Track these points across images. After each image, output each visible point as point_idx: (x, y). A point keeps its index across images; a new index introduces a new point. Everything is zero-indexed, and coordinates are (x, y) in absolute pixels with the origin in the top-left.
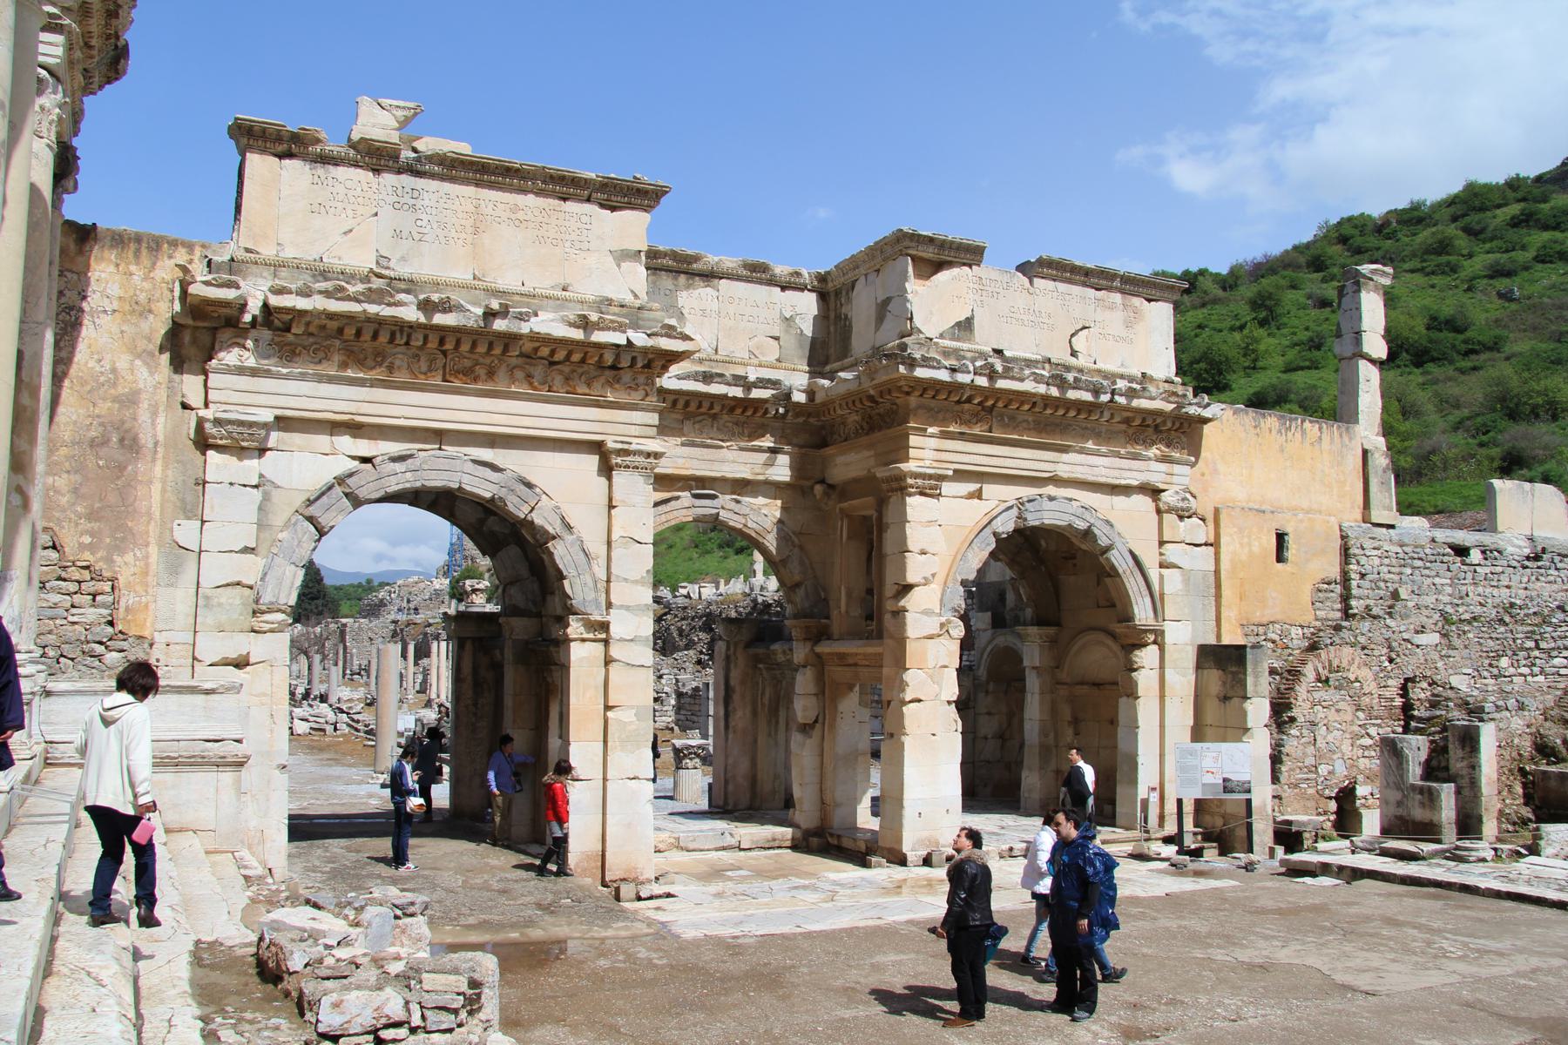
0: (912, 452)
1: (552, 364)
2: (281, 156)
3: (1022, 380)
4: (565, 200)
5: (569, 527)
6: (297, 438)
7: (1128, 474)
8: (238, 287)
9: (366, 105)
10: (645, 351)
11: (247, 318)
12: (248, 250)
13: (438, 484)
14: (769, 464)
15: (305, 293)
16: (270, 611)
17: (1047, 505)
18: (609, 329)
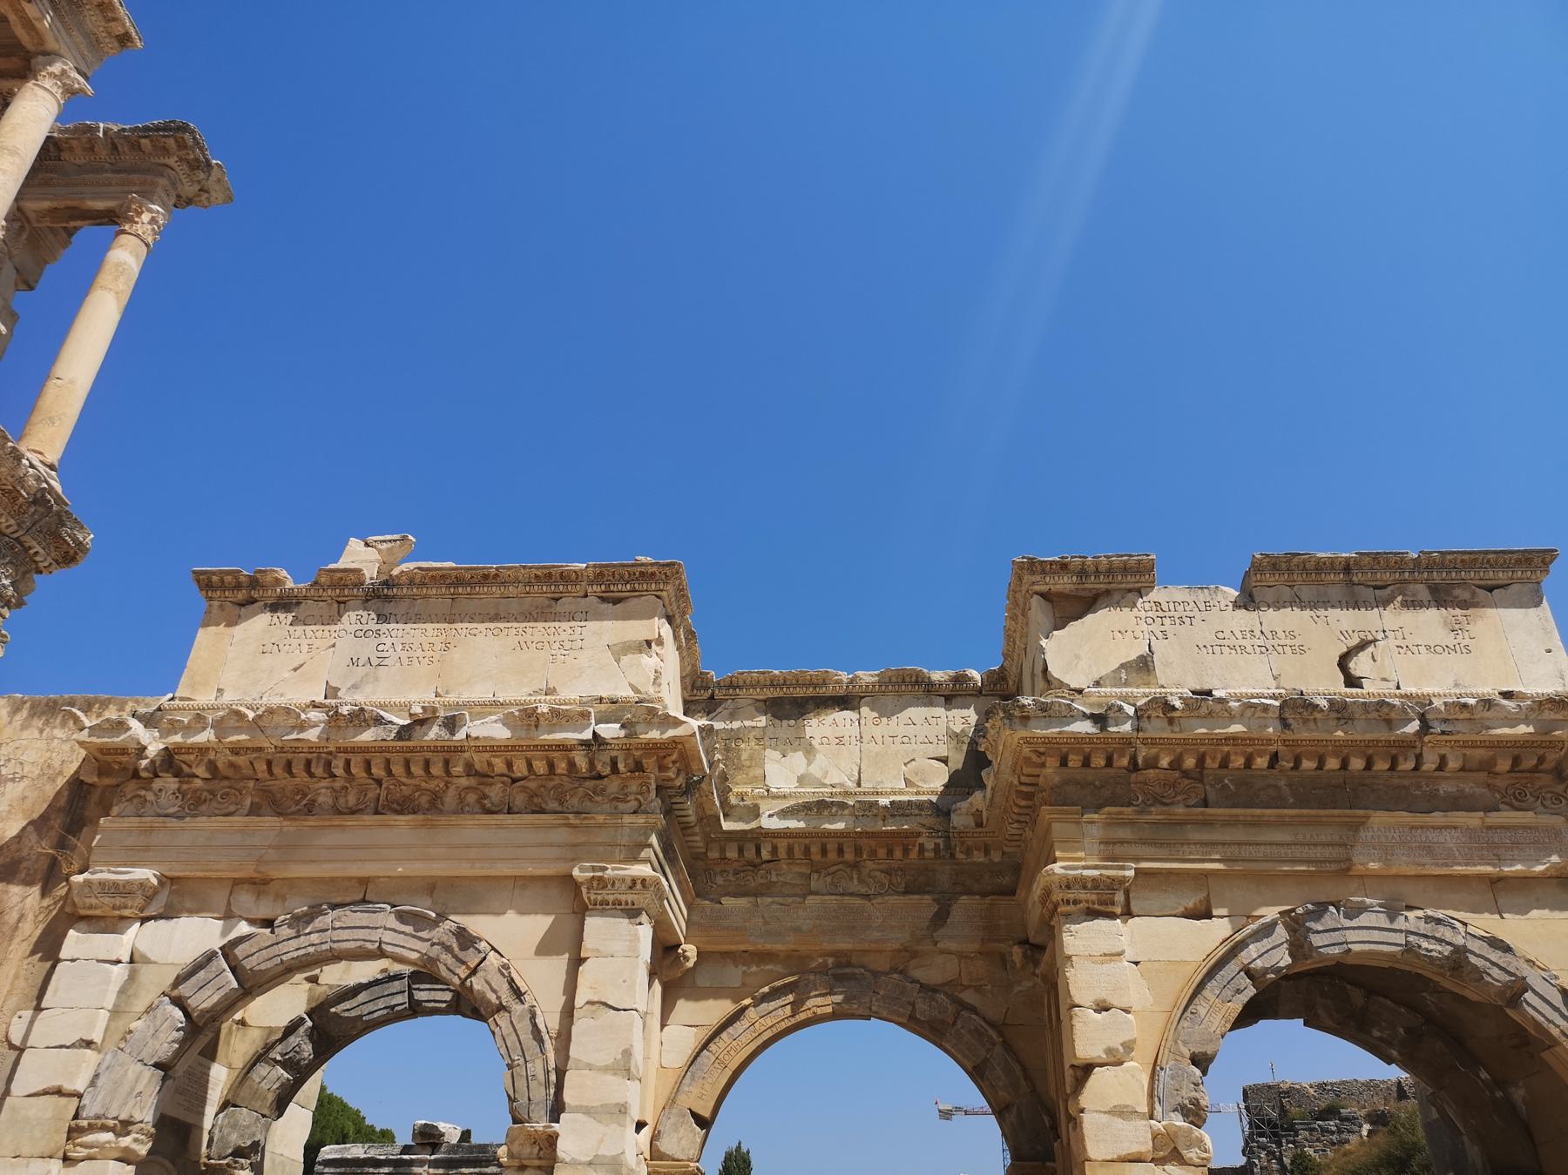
1: (514, 781)
5: (518, 994)
9: (355, 544)
16: (92, 1128)
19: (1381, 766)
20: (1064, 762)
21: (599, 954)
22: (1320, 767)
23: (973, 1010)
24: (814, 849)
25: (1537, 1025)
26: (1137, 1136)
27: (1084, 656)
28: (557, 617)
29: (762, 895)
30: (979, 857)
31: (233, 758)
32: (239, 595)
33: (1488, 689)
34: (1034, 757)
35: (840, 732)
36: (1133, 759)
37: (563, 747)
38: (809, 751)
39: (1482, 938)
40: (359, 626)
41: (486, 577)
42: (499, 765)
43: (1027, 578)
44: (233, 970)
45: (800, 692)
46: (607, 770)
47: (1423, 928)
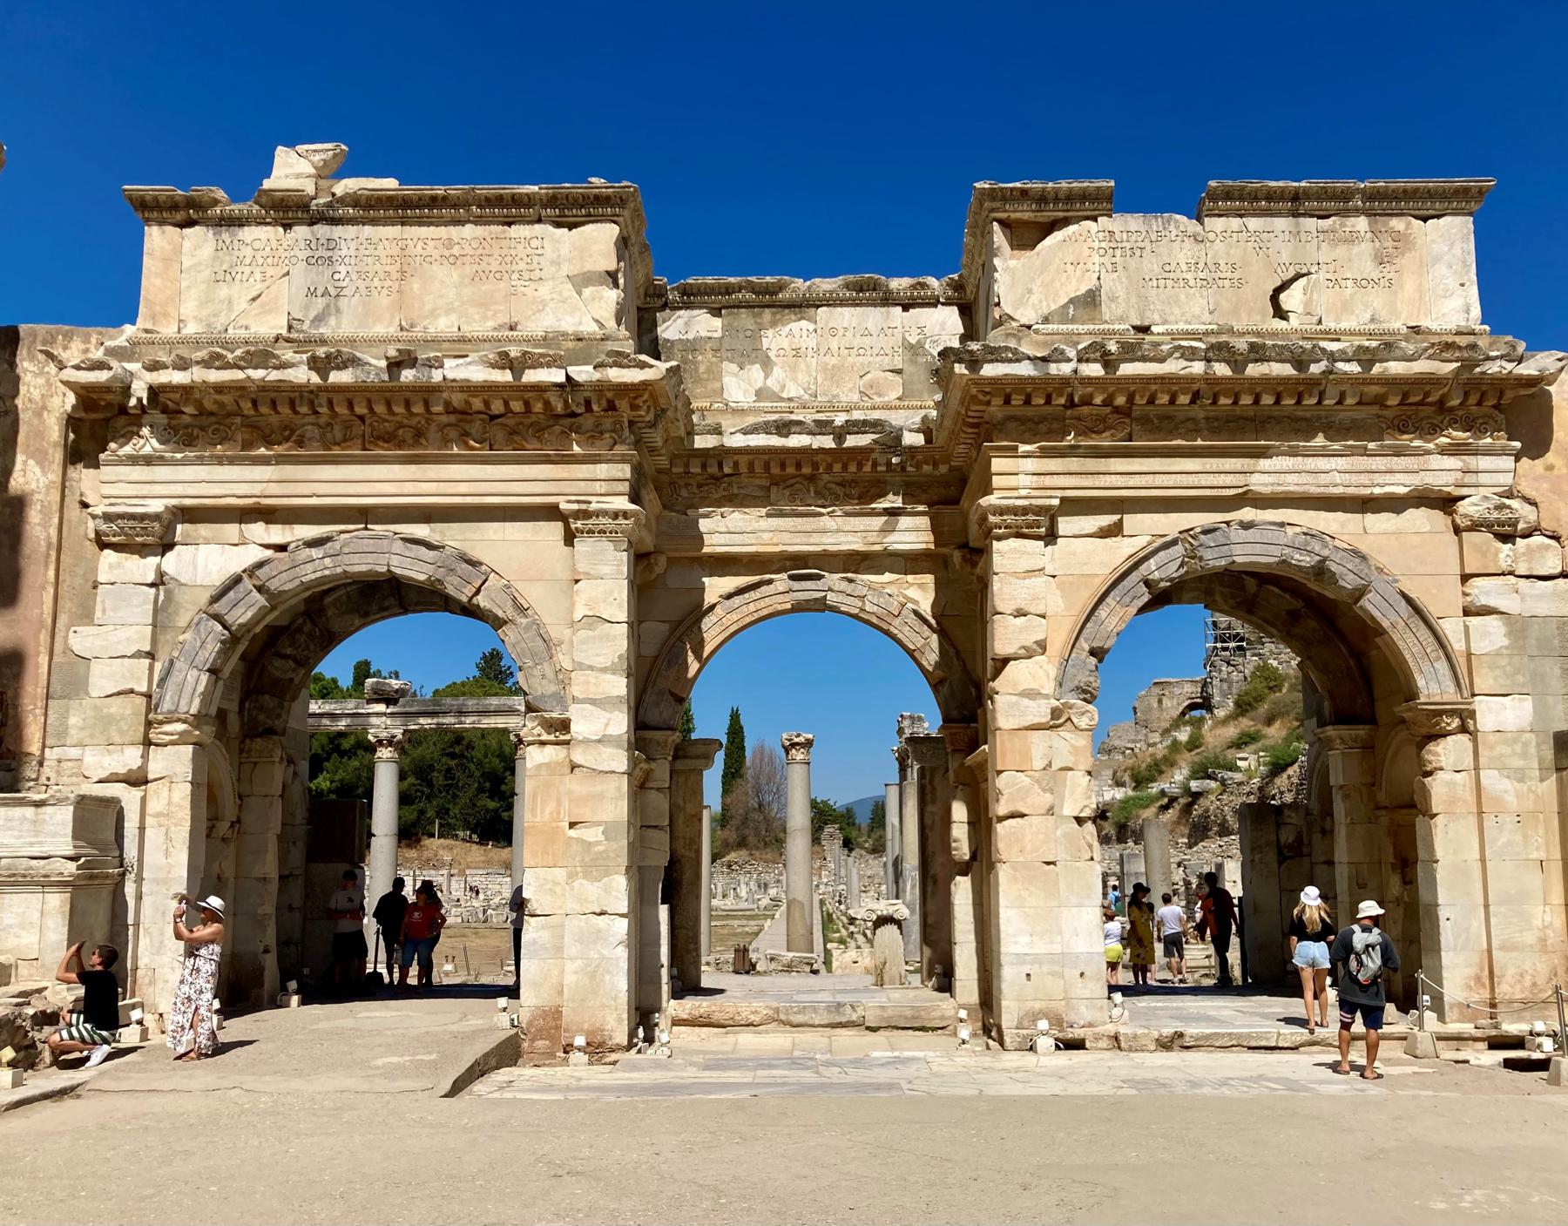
0: (997, 481)
1: (493, 418)
2: (182, 225)
3: (1162, 360)
4: (509, 224)
5: (522, 610)
6: (203, 530)
7: (1388, 478)
8: (110, 368)
10: (601, 388)
11: (133, 402)
12: (147, 331)
13: (363, 568)
14: (887, 530)
15: (182, 365)
16: (169, 722)
17: (1237, 534)
18: (541, 366)
20: (1007, 401)
21: (589, 576)
22: (1235, 403)
25: (1373, 618)
26: (1039, 711)
30: (927, 468)
31: (217, 397)
33: (1398, 325)
34: (981, 397)
35: (797, 342)
36: (1071, 397)
37: (539, 388)
38: (767, 364)
39: (1345, 550)
40: (309, 253)
42: (477, 404)
44: (260, 589)
46: (581, 410)
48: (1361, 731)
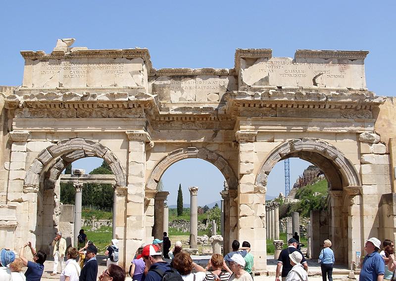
0: (241, 127)
1: (109, 109)
5: (116, 159)
16: (28, 186)
19: (317, 107)
20: (244, 106)
21: (133, 151)
22: (303, 107)
23: (222, 157)
24: (184, 119)
26: (251, 189)
27: (251, 76)
28: (115, 63)
29: (170, 129)
32: (32, 58)
33: (345, 88)
34: (237, 104)
36: (260, 105)
38: (182, 91)
41: (96, 53)
42: (105, 106)
43: (239, 54)
45: (179, 74)
46: (132, 107)
47: (319, 144)
48: (338, 192)
